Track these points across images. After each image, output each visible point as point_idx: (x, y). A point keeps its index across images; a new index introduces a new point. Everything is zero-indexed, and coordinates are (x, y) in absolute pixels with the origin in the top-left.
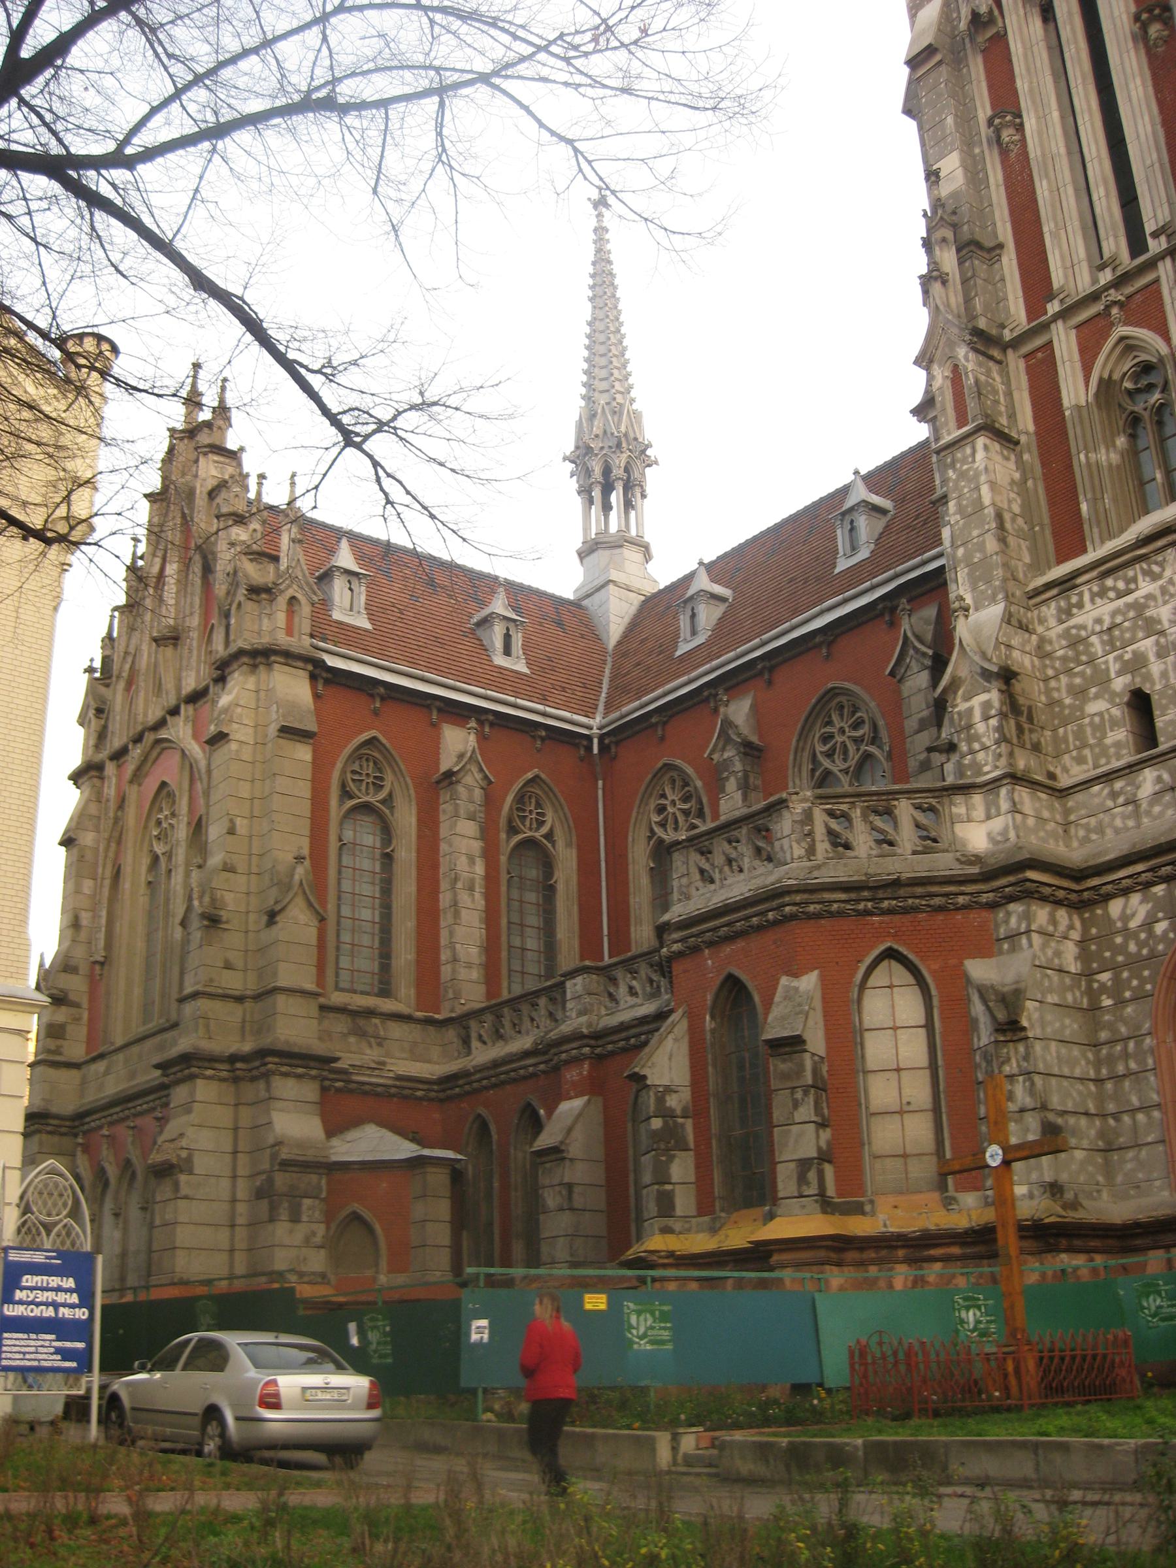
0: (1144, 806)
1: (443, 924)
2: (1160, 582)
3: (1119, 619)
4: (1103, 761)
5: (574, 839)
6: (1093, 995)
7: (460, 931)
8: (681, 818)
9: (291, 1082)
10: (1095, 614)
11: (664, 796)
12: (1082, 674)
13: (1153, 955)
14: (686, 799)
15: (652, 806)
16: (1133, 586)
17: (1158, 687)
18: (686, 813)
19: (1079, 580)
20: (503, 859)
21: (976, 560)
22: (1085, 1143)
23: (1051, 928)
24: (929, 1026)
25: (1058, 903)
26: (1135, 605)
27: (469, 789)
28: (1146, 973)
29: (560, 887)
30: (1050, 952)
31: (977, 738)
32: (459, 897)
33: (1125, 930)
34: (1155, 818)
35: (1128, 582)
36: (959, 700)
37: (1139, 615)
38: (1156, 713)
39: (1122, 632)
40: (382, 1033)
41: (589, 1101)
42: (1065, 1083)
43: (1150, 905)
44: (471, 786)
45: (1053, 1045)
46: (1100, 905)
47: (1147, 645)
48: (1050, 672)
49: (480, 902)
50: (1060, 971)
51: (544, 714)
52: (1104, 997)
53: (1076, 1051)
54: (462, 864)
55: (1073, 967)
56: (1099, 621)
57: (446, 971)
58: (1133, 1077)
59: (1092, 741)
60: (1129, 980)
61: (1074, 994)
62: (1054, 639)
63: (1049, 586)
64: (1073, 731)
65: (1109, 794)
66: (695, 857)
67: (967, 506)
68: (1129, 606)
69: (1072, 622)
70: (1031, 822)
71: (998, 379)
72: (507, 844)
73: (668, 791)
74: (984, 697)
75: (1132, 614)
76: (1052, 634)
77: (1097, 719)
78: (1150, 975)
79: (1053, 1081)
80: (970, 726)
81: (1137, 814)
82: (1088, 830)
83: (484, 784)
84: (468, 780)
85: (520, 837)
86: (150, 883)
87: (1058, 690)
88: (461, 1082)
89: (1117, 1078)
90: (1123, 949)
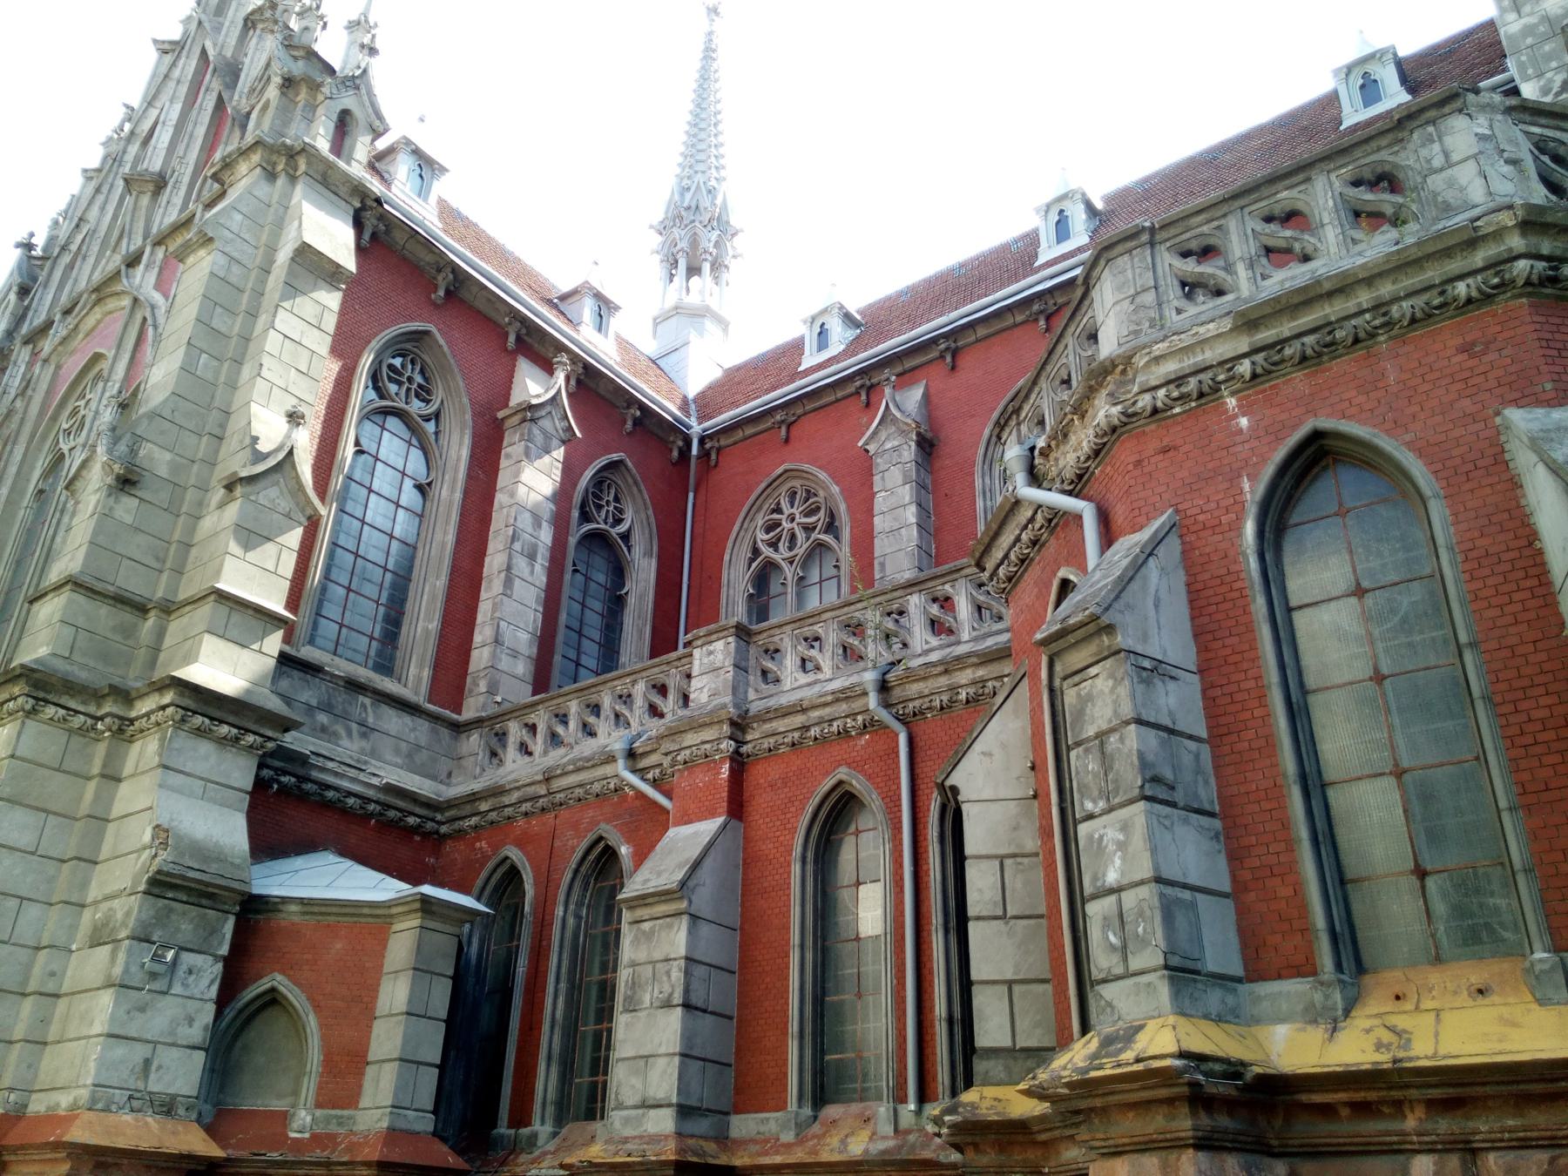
1: (483, 595)
5: (655, 548)
7: (509, 607)
8: (800, 535)
9: (205, 747)
11: (778, 510)
14: (810, 513)
15: (760, 523)
18: (808, 529)
20: (573, 541)
29: (632, 601)
32: (514, 561)
40: (371, 720)
41: (724, 827)
49: (541, 578)
66: (1169, 261)
73: (785, 505)
84: (546, 424)
85: (594, 526)
86: (41, 492)
88: (484, 807)
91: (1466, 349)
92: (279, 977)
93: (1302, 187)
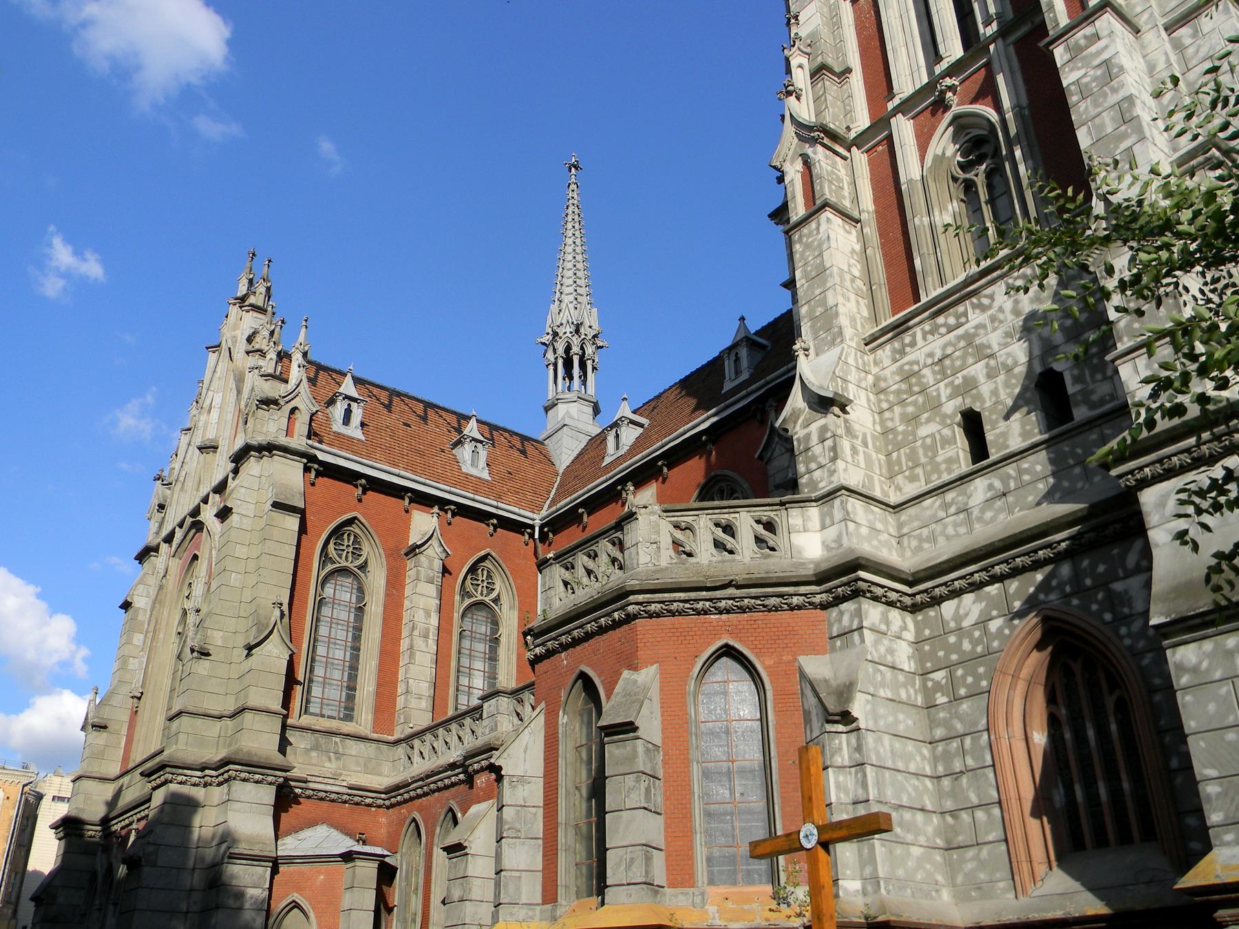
0: (976, 512)
1: (401, 664)
2: (990, 313)
4: (934, 477)
6: (928, 693)
10: (927, 349)
12: (915, 403)
13: (989, 652)
16: (963, 320)
17: (988, 404)
21: (818, 314)
22: (922, 840)
23: (883, 627)
24: (764, 719)
25: (891, 604)
27: (431, 560)
28: (981, 670)
30: (882, 649)
34: (987, 523)
35: (958, 317)
37: (970, 344)
38: (987, 427)
39: (953, 361)
42: (900, 777)
44: (432, 557)
45: (886, 738)
47: (978, 370)
48: (885, 405)
49: (433, 647)
50: (893, 668)
51: (497, 507)
52: (938, 695)
53: (910, 746)
54: (420, 616)
55: (908, 665)
56: (931, 355)
57: (400, 702)
58: (970, 773)
59: (923, 460)
60: (964, 677)
61: (907, 691)
62: (889, 376)
64: (905, 453)
65: (940, 507)
68: (959, 338)
69: (907, 359)
70: (864, 531)
71: (843, 171)
72: (459, 605)
75: (962, 344)
76: (887, 373)
77: (929, 441)
78: (986, 672)
79: (887, 773)
81: (969, 522)
82: (920, 539)
83: (443, 556)
84: (430, 552)
85: (475, 599)
87: (892, 420)
89: (956, 776)
90: (957, 648)
92: (296, 894)
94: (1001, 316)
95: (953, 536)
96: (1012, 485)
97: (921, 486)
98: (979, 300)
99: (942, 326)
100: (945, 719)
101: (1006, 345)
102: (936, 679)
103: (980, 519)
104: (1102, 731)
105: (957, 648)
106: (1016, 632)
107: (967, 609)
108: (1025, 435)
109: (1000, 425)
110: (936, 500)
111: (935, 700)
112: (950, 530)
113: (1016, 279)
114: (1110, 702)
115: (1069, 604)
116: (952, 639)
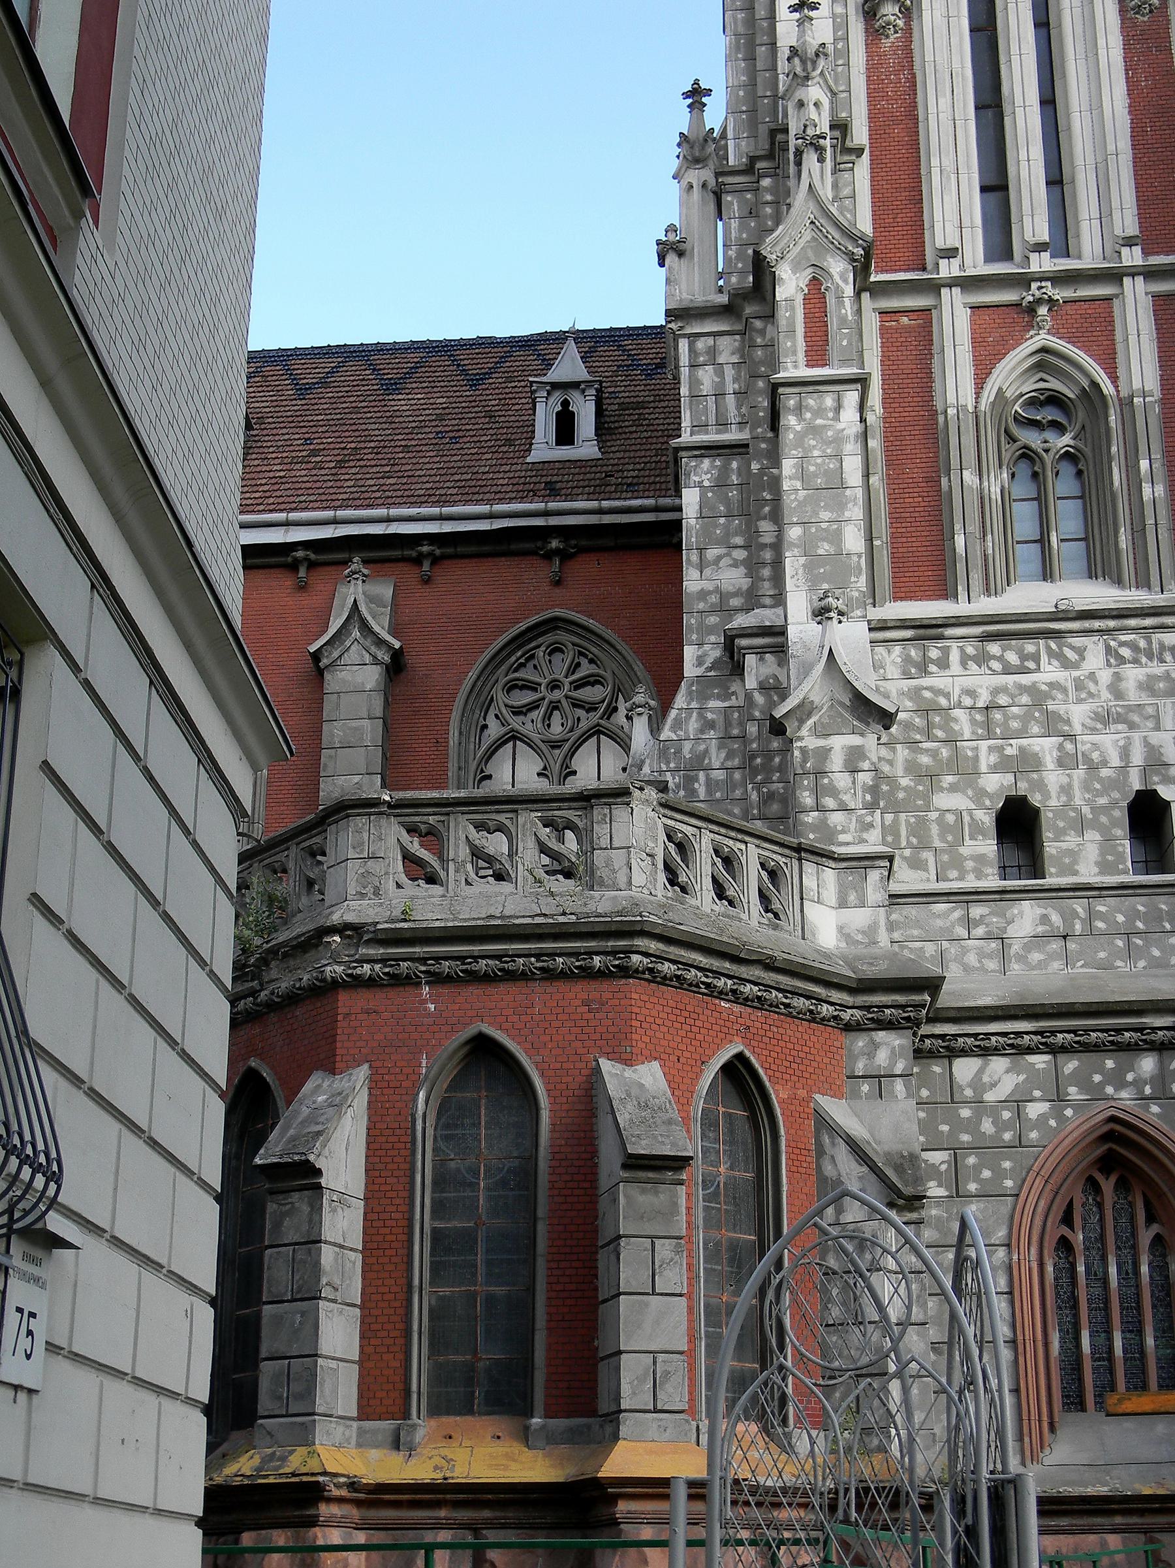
0: (1016, 948)
2: (1076, 673)
3: (1003, 700)
4: (953, 874)
10: (968, 682)
12: (934, 754)
17: (1053, 802)
19: (949, 632)
21: (821, 552)
26: (1032, 690)
31: (833, 792)
33: (978, 1102)
35: (1024, 657)
36: (804, 732)
43: (1022, 1078)
46: (940, 1061)
47: (1045, 747)
56: (971, 693)
63: (903, 624)
67: (815, 475)
68: (1023, 689)
74: (855, 740)
77: (950, 818)
80: (820, 773)
81: (1003, 955)
90: (972, 1126)
91: (586, 1003)
93: (509, 815)
94: (1092, 687)
95: (977, 969)
96: (1078, 927)
97: (928, 880)
98: (1060, 648)
99: (994, 657)
100: (938, 1218)
101: (1094, 731)
102: (931, 1161)
103: (1021, 959)
104: (1130, 1274)
105: (972, 1126)
106: (1069, 1128)
107: (996, 1078)
108: (1105, 867)
109: (1068, 838)
110: (954, 910)
111: (925, 1190)
112: (972, 959)
113: (1122, 644)
114: (1145, 1237)
115: (1147, 1108)
116: (965, 1113)
